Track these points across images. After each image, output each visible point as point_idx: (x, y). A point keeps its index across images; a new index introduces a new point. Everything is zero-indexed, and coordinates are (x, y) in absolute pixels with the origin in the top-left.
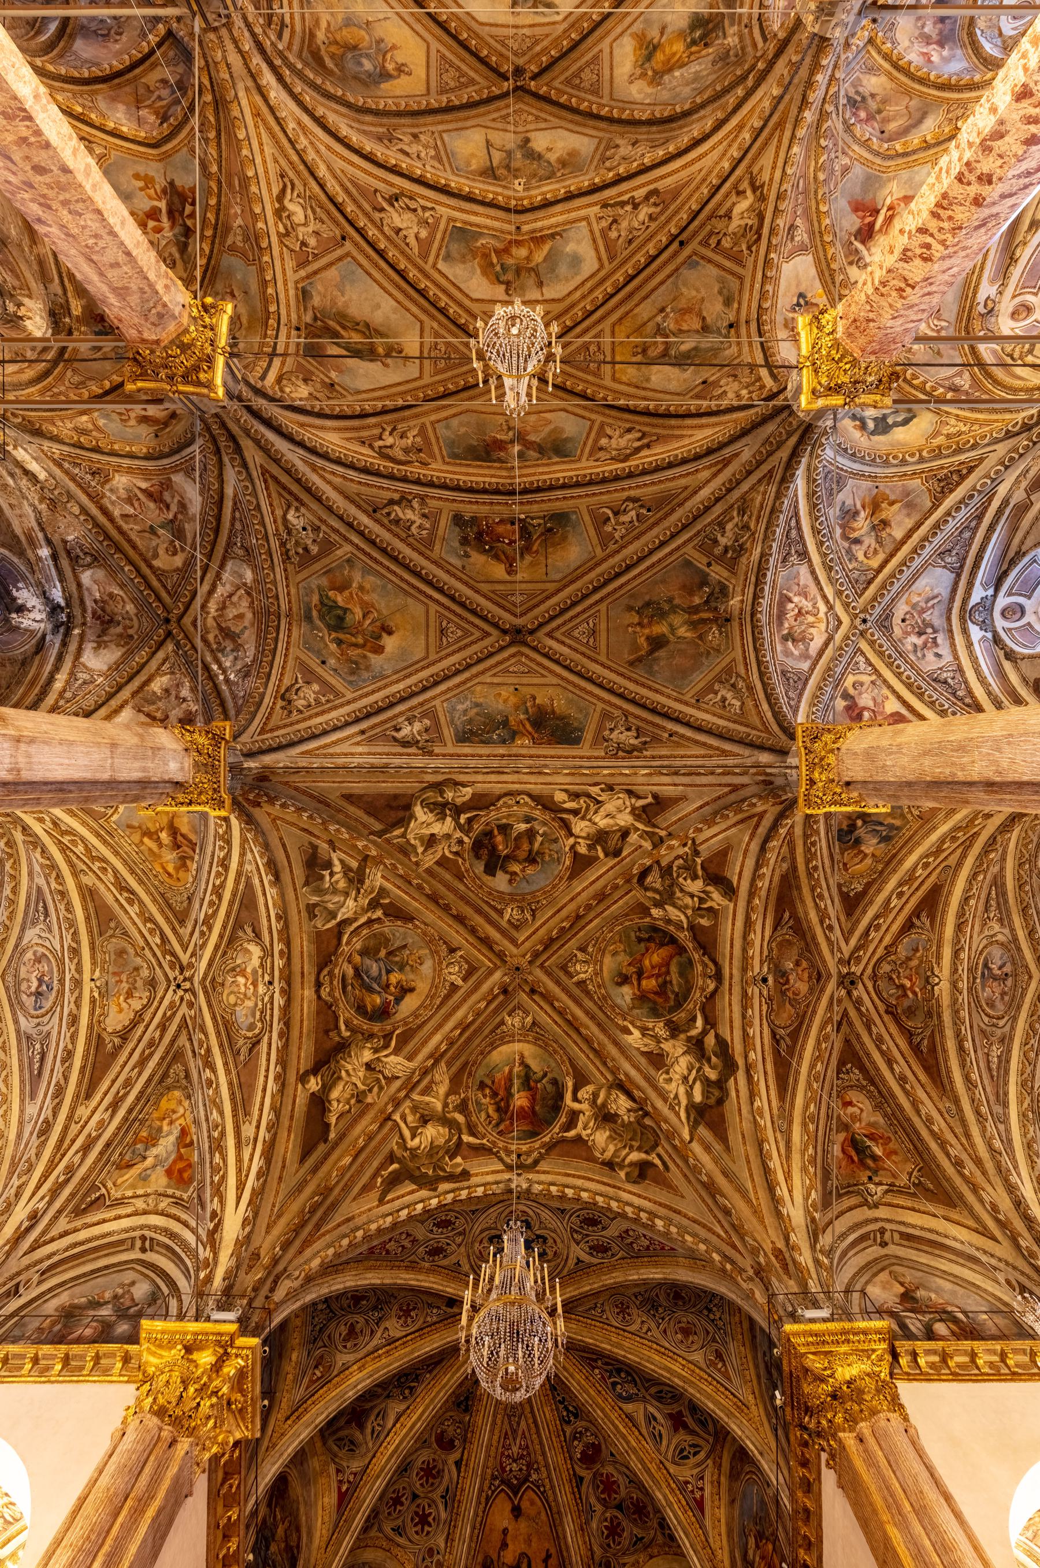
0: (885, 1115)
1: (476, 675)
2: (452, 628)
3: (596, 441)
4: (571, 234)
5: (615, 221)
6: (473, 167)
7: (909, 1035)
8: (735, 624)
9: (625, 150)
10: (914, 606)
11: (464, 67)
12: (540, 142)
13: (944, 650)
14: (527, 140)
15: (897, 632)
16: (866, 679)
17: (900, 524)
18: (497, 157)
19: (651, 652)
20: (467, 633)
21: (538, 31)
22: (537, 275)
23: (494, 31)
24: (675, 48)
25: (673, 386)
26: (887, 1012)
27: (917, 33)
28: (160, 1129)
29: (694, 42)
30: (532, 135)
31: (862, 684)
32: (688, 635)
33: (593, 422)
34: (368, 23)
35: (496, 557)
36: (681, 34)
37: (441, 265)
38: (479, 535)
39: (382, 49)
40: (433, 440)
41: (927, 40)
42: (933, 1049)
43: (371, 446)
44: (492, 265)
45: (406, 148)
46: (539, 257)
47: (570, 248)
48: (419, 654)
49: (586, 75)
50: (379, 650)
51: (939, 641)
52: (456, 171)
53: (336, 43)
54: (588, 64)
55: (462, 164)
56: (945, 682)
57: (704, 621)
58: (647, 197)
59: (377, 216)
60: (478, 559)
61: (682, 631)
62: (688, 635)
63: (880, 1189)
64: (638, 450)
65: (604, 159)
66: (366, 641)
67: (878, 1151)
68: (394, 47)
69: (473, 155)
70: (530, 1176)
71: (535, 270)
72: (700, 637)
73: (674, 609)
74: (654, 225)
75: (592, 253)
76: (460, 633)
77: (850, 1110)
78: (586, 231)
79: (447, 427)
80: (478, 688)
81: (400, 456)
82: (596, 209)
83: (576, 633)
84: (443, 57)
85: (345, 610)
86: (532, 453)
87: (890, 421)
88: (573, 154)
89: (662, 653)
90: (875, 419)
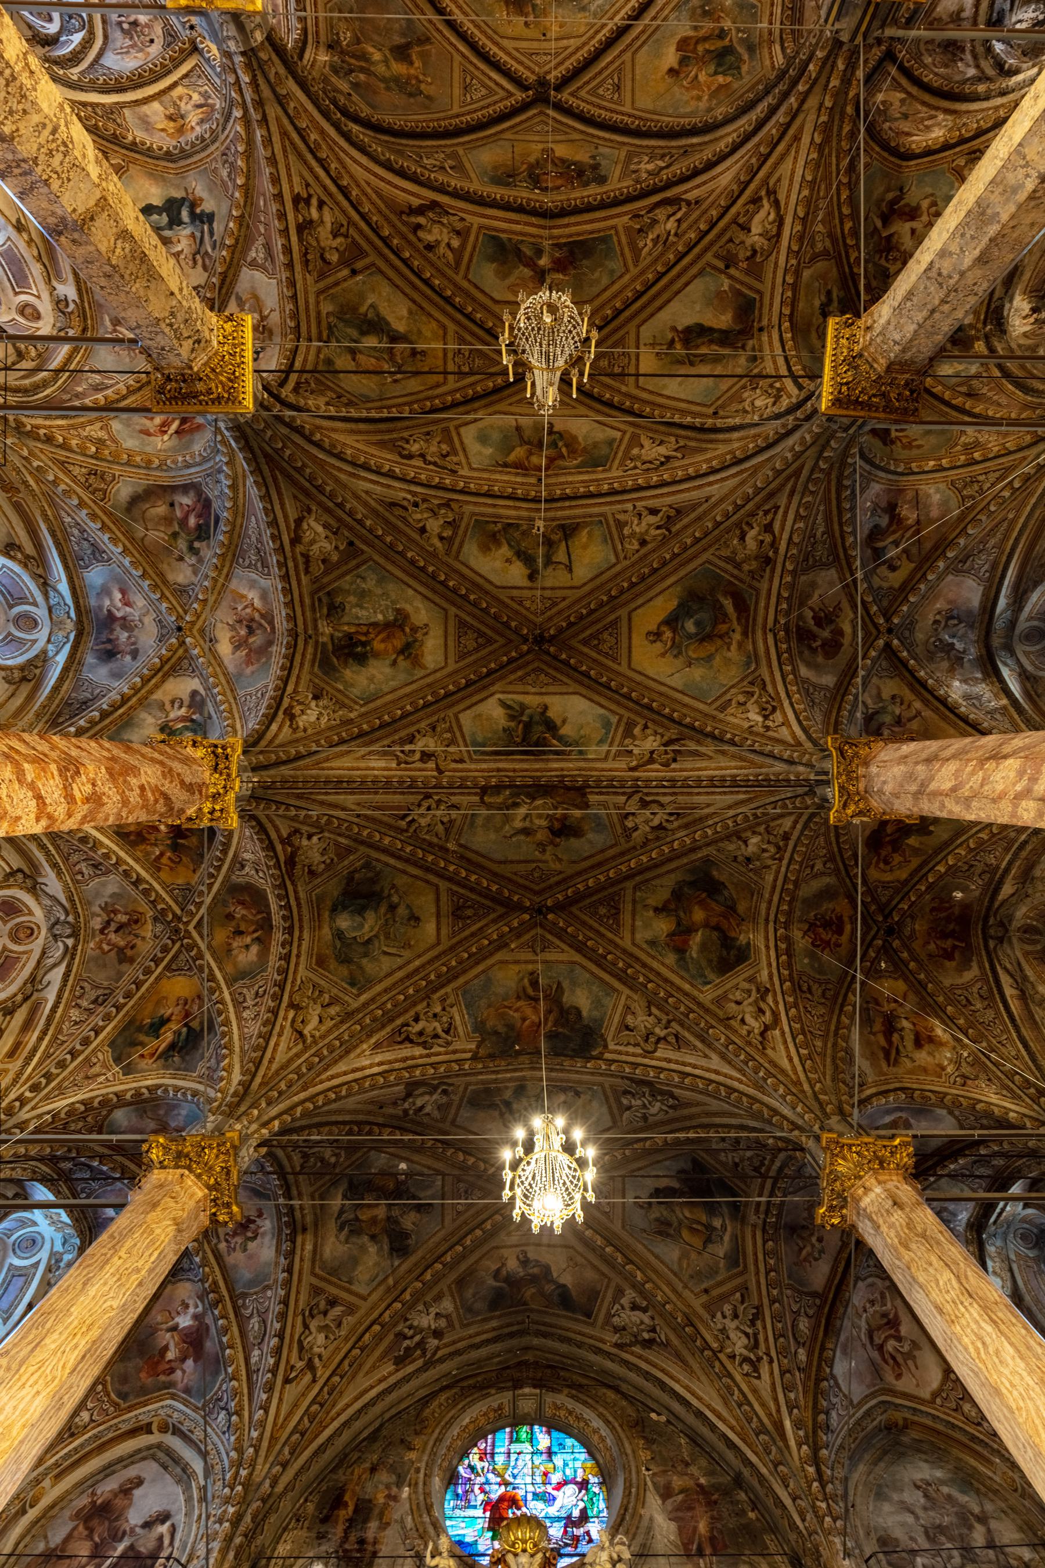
1: (584, 44)
2: (608, 95)
3: (463, 246)
4: (487, 462)
5: (445, 456)
6: (585, 533)
8: (323, 38)
9: (434, 526)
10: (141, 50)
11: (594, 655)
12: (516, 573)
14: (531, 577)
17: (156, 113)
18: (561, 556)
19: (407, 46)
20: (593, 92)
21: (520, 688)
22: (521, 437)
23: (564, 689)
24: (382, 646)
25: (386, 289)
27: (136, 632)
29: (364, 644)
30: (526, 583)
32: (371, 50)
33: (466, 277)
34: (690, 665)
35: (563, 161)
36: (376, 655)
37: (618, 435)
38: (580, 173)
39: (676, 649)
40: (627, 250)
41: (126, 624)
43: (689, 203)
44: (567, 446)
45: (652, 519)
46: (519, 453)
47: (488, 451)
48: (642, 56)
49: (471, 645)
50: (683, 44)
52: (602, 520)
53: (721, 637)
54: (470, 653)
55: (597, 532)
57: (354, 56)
58: (410, 457)
59: (682, 443)
60: (582, 156)
61: (377, 56)
62: (371, 50)
64: (421, 211)
65: (453, 524)
66: (694, 51)
68: (663, 655)
69: (585, 547)
71: (523, 442)
72: (359, 42)
73: (383, 80)
74: (405, 434)
75: (466, 441)
76: (601, 91)
78: (472, 459)
79: (612, 272)
80: (583, 29)
81: (660, 214)
82: (461, 472)
83: (484, 92)
84: (614, 659)
85: (716, 73)
86: (528, 251)
88: (485, 549)
89: (398, 40)
90: (180, 223)
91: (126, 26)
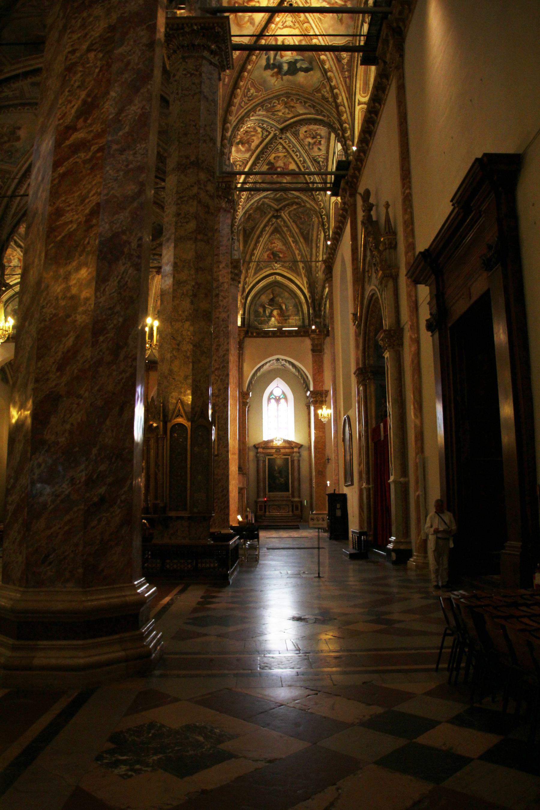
0: (286, 247)
7: (300, 229)
13: (323, 148)
15: (301, 136)
16: (281, 155)
26: (293, 222)
28: (10, 258)
31: (279, 157)
42: (308, 234)
50: (18, 139)
51: (322, 142)
56: (319, 163)
63: (278, 266)
67: (281, 255)
70: (154, 252)
77: (273, 245)
87: (298, 65)
91: (319, 137)
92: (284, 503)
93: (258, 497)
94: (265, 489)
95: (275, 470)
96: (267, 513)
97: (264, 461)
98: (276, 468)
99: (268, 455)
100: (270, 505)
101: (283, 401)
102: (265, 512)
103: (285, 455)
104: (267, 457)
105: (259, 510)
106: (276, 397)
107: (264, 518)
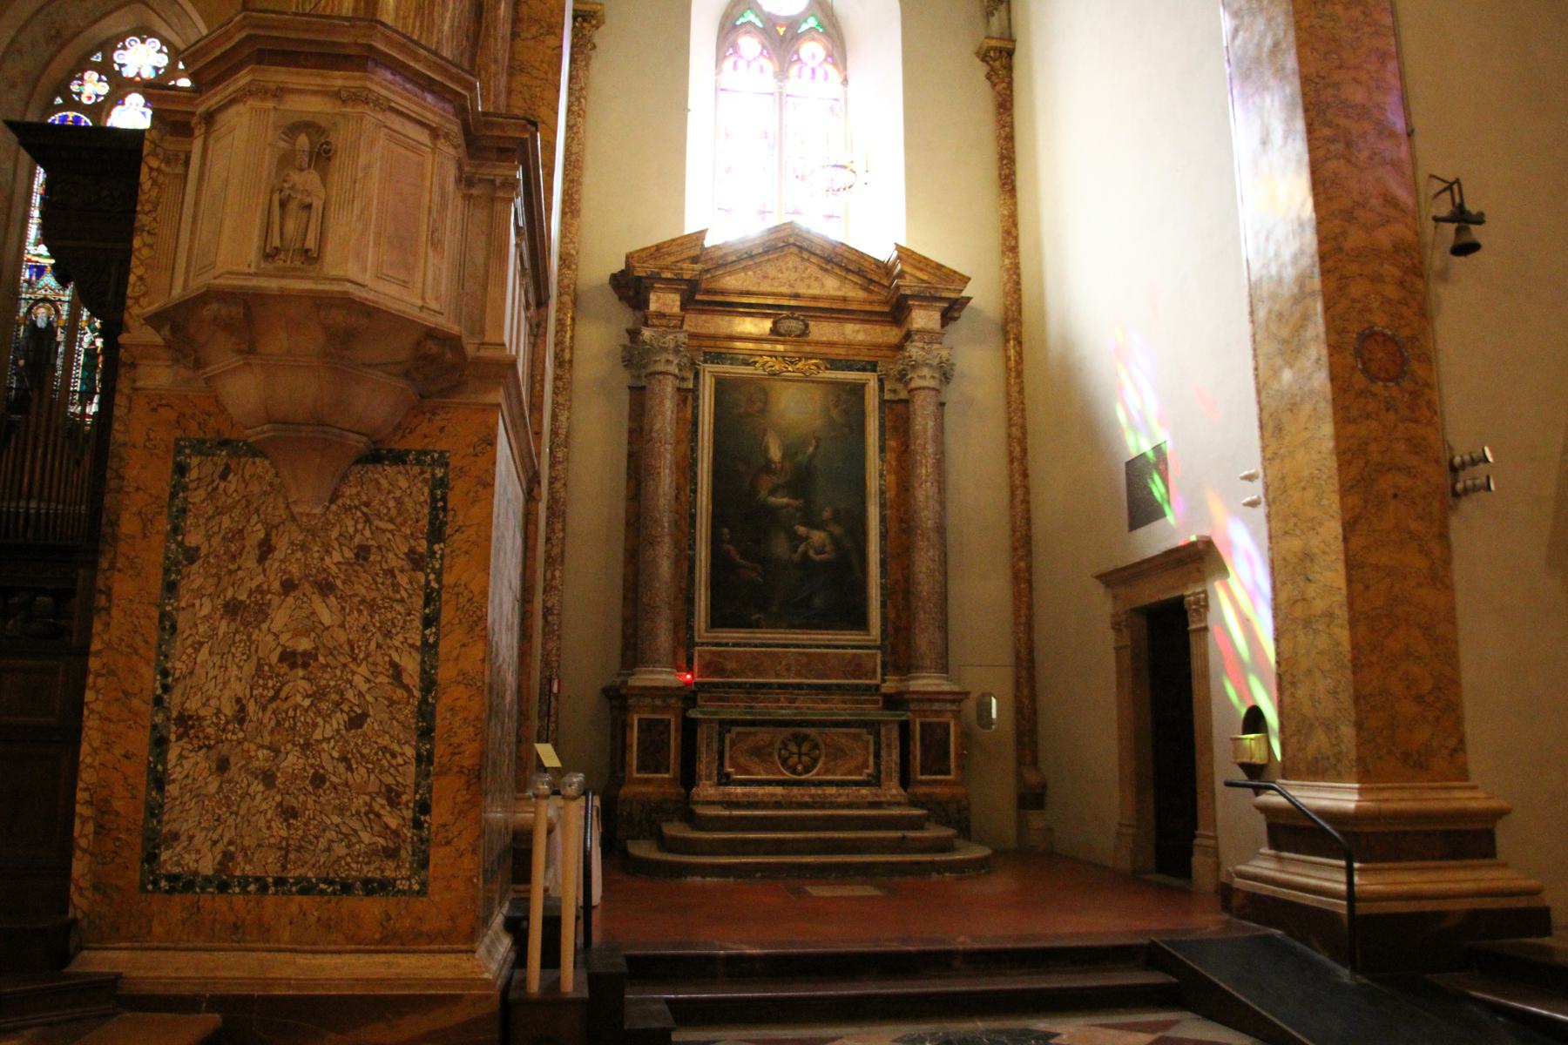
92: (840, 708)
93: (633, 652)
94: (690, 601)
95: (767, 467)
96: (706, 789)
97: (688, 397)
98: (775, 453)
99: (718, 358)
100: (726, 725)
101: (812, 50)
102: (689, 778)
103: (834, 364)
104: (709, 368)
105: (633, 758)
106: (770, 22)
107: (674, 829)
